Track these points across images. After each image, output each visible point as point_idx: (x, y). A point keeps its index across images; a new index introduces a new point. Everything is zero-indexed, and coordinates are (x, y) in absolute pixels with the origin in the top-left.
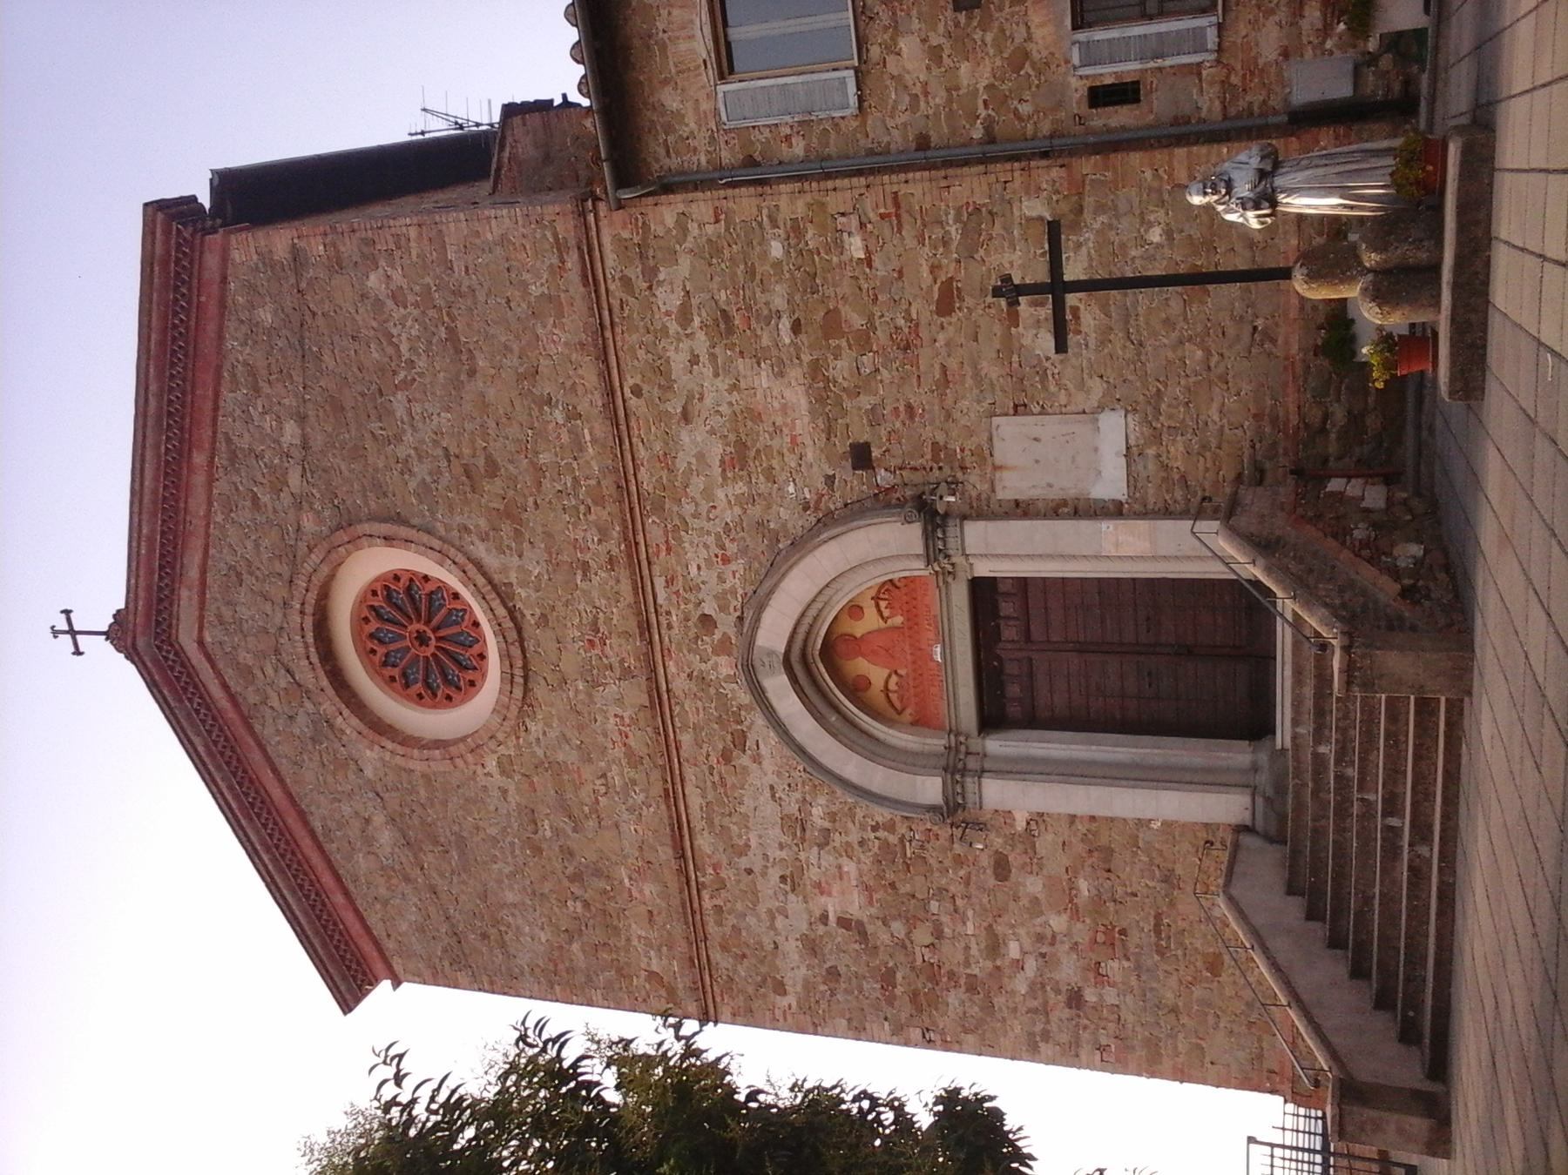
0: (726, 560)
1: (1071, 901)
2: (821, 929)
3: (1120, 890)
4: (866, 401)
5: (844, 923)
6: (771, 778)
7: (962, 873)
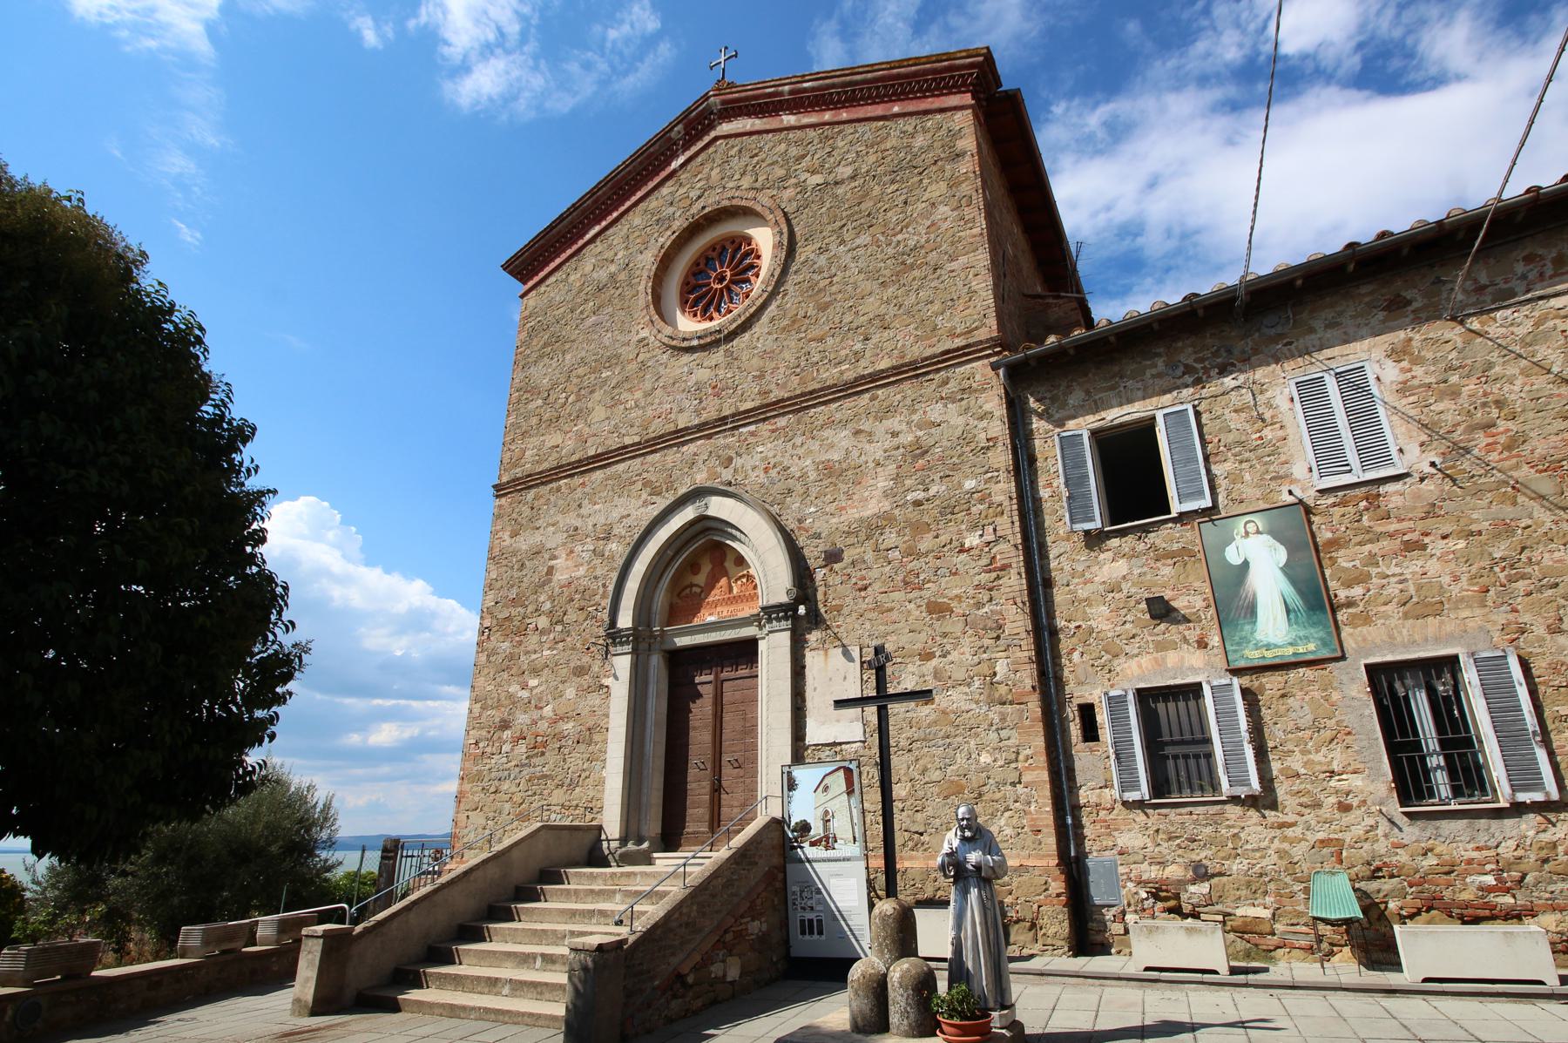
0: (766, 470)
2: (547, 556)
5: (550, 571)
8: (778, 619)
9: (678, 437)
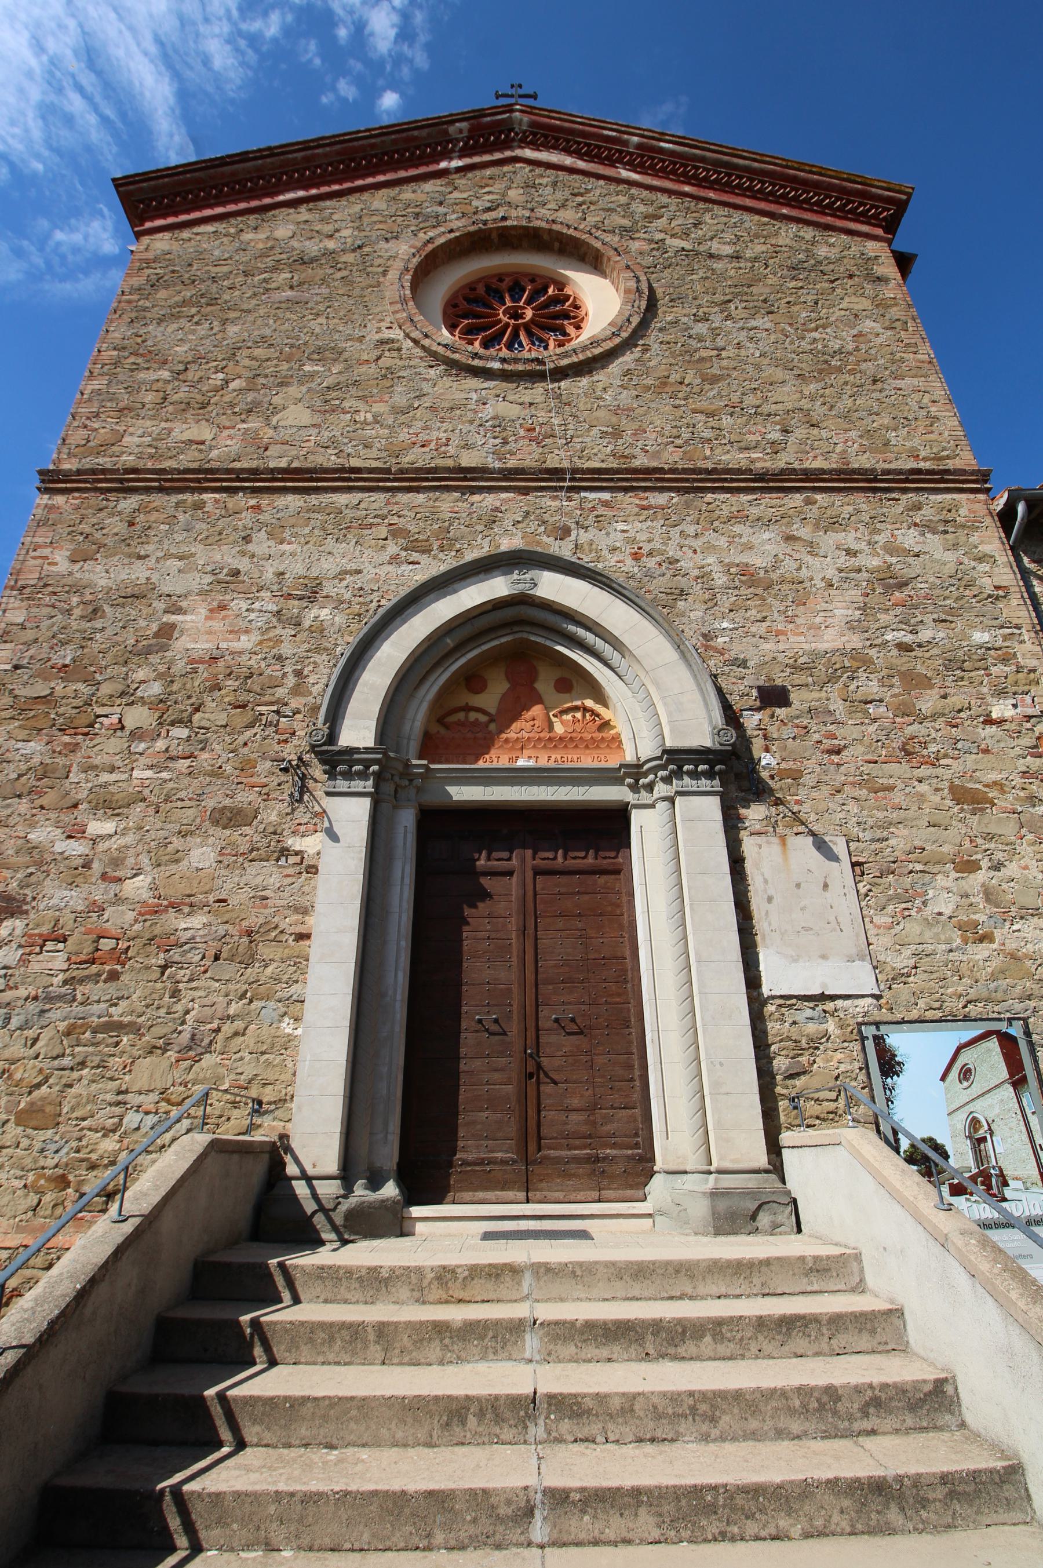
0: (636, 556)
1: (172, 905)
2: (160, 605)
3: (183, 974)
4: (837, 706)
5: (167, 631)
6: (369, 572)
7: (228, 769)
8: (695, 775)
9: (467, 479)
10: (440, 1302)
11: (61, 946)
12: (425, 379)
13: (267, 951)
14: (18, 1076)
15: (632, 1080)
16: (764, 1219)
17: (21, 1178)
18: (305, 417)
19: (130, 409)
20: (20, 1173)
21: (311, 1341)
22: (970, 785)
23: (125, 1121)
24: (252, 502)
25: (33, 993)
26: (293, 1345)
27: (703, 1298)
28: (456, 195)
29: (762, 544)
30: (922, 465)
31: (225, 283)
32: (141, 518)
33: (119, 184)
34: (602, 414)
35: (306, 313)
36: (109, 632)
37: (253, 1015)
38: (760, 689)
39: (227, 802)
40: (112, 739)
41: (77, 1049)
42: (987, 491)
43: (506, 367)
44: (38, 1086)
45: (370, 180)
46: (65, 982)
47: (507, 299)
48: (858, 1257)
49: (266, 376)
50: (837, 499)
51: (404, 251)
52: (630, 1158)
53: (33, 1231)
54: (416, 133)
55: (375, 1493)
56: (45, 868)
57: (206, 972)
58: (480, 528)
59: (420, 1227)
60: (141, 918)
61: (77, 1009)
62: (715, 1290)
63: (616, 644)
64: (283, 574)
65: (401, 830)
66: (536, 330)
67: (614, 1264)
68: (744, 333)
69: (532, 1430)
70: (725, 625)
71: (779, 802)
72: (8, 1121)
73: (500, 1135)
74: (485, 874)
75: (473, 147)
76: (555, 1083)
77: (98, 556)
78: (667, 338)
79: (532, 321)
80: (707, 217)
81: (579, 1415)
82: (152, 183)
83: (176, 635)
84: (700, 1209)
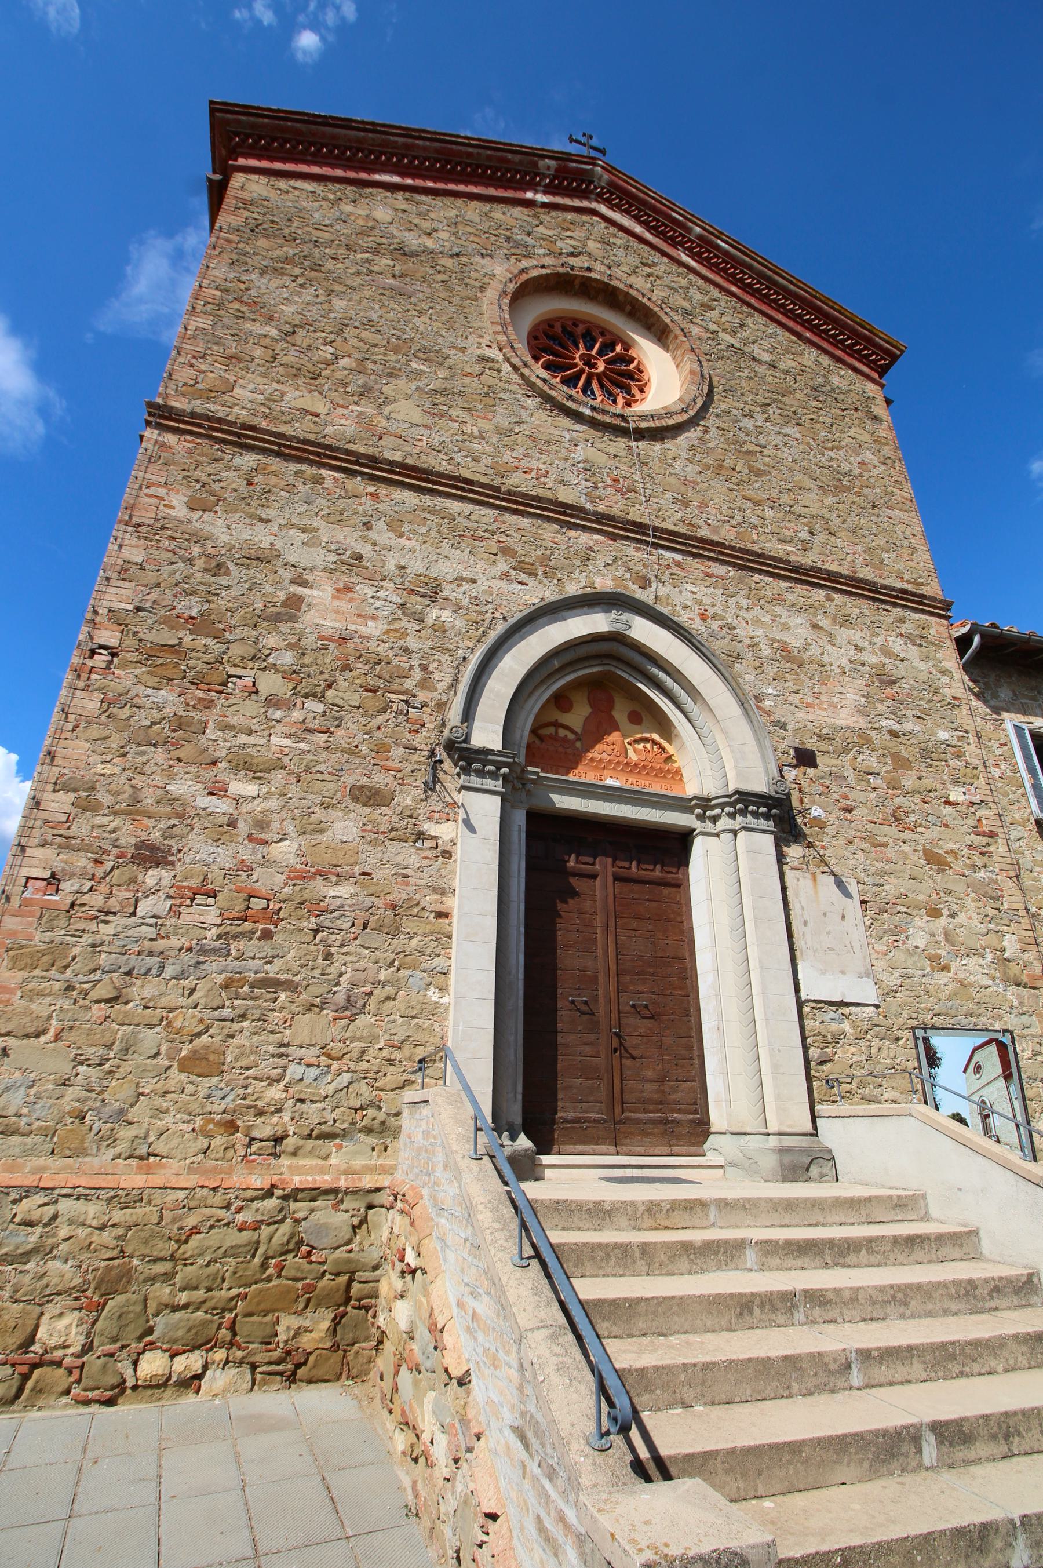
0: (703, 617)
1: (319, 873)
2: (287, 575)
3: (335, 939)
4: (849, 773)
6: (484, 584)
7: (364, 749)
8: (756, 815)
9: (566, 514)
10: (651, 1229)
11: (211, 901)
12: (524, 407)
13: (411, 925)
14: (178, 1024)
15: (691, 1058)
16: (814, 1171)
17: (189, 1122)
18: (417, 416)
19: (239, 360)
20: (187, 1118)
21: (592, 1258)
22: (936, 851)
23: (288, 1072)
24: (371, 489)
25: (187, 945)
26: (579, 1262)
27: (831, 1225)
28: (541, 229)
29: (796, 627)
30: (905, 586)
31: (327, 251)
32: (259, 479)
33: (214, 108)
34: (672, 480)
35: (411, 307)
36: (235, 591)
37: (402, 982)
38: (796, 749)
39: (365, 781)
40: (248, 702)
41: (237, 1002)
42: (948, 618)
43: (595, 415)
44: (199, 1035)
45: (461, 188)
46: (219, 937)
47: (581, 345)
48: (924, 1196)
49: (375, 363)
50: (849, 601)
51: (501, 271)
52: (692, 1121)
53: (206, 1172)
54: (510, 156)
55: (750, 1360)
56: (189, 821)
57: (355, 939)
58: (578, 563)
59: (548, 1172)
60: (290, 882)
61: (231, 963)
62: (838, 1220)
63: (693, 691)
64: (404, 568)
65: (516, 828)
66: (606, 383)
67: (771, 1200)
68: (780, 437)
69: (796, 1315)
70: (770, 691)
71: (810, 845)
72: (170, 1067)
73: (592, 1098)
74: (575, 875)
75: (557, 187)
76: (634, 1058)
77: (217, 509)
78: (722, 425)
79: (604, 373)
80: (749, 321)
81: (825, 1304)
82: (252, 119)
83: (304, 608)
84: (769, 1162)
